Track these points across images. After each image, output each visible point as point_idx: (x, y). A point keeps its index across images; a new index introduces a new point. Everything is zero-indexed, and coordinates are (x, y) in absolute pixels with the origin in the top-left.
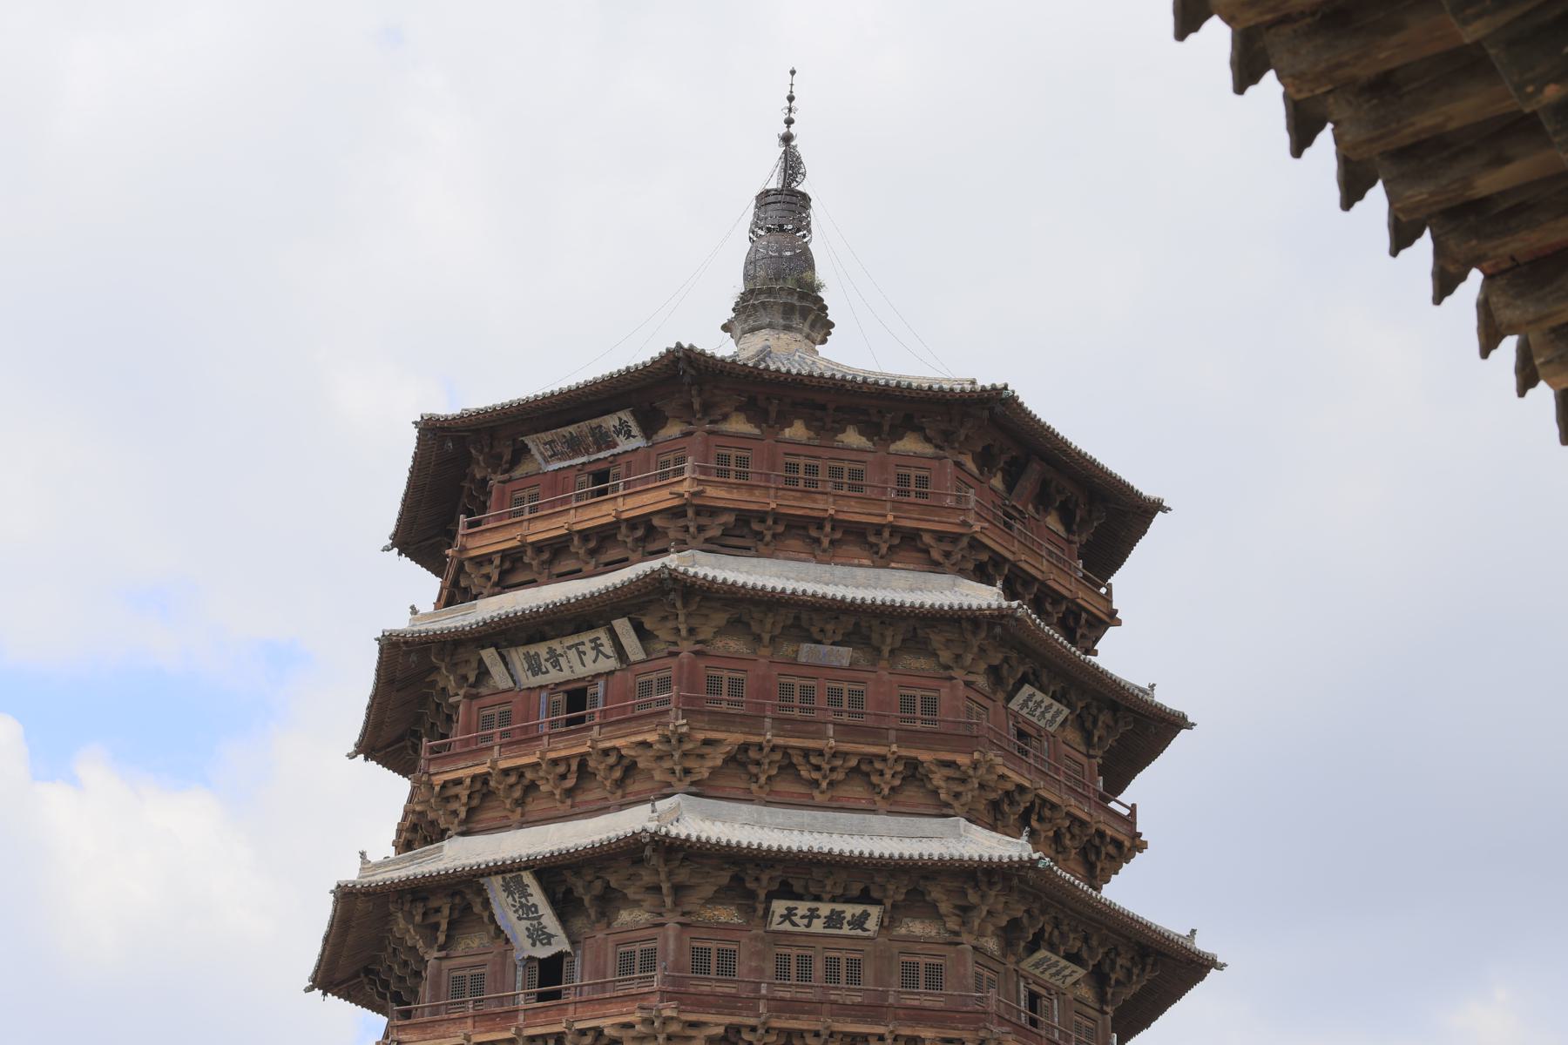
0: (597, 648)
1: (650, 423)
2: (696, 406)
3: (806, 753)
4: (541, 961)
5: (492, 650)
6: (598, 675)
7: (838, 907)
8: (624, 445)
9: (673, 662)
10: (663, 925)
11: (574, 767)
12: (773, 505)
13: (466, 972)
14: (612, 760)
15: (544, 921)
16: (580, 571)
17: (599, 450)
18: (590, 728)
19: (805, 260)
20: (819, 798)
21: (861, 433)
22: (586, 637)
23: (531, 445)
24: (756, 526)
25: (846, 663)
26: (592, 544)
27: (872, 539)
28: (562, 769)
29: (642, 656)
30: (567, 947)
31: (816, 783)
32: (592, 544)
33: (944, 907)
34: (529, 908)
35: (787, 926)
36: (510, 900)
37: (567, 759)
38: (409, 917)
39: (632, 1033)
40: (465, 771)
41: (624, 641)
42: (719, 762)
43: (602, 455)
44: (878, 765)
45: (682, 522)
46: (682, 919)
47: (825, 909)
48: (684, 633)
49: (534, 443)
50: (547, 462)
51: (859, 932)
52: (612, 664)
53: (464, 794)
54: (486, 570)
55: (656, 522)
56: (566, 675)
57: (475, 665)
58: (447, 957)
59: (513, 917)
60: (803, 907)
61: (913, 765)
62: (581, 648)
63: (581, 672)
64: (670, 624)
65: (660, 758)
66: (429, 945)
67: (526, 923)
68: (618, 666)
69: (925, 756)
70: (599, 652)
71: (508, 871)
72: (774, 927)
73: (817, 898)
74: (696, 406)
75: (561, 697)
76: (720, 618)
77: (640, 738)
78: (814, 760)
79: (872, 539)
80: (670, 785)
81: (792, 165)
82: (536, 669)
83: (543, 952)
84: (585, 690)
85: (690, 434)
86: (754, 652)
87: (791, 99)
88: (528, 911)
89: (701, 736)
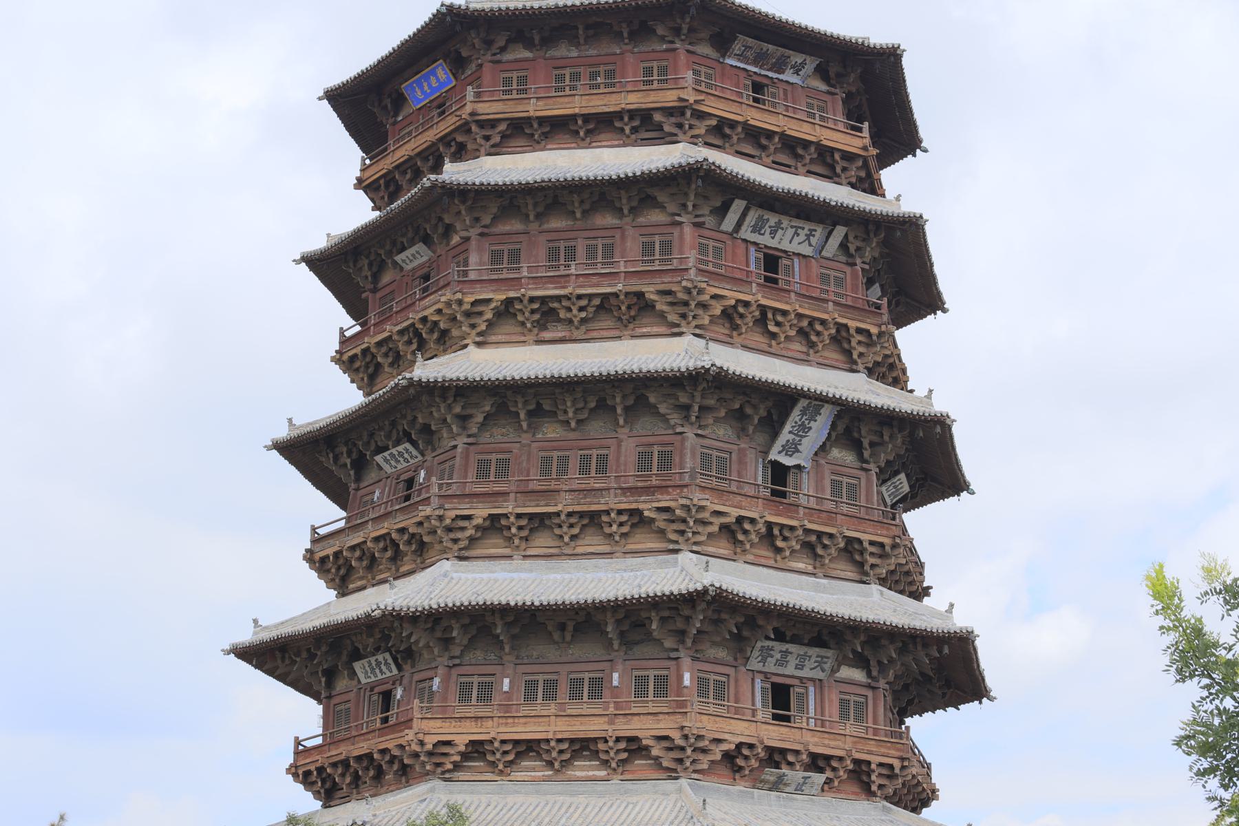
0: (808, 237)
4: (776, 465)
5: (744, 203)
6: (799, 255)
8: (789, 76)
9: (848, 270)
10: (867, 470)
13: (715, 453)
15: (804, 440)
16: (753, 157)
18: (826, 301)
22: (808, 226)
36: (797, 419)
37: (800, 316)
38: (703, 397)
40: (732, 295)
41: (830, 240)
43: (770, 74)
45: (845, 164)
52: (806, 250)
62: (800, 231)
63: (785, 245)
64: (859, 244)
65: (859, 342)
67: (791, 437)
70: (808, 239)
71: (819, 400)
75: (761, 256)
80: (855, 363)
83: (788, 461)
84: (777, 259)
88: (803, 429)
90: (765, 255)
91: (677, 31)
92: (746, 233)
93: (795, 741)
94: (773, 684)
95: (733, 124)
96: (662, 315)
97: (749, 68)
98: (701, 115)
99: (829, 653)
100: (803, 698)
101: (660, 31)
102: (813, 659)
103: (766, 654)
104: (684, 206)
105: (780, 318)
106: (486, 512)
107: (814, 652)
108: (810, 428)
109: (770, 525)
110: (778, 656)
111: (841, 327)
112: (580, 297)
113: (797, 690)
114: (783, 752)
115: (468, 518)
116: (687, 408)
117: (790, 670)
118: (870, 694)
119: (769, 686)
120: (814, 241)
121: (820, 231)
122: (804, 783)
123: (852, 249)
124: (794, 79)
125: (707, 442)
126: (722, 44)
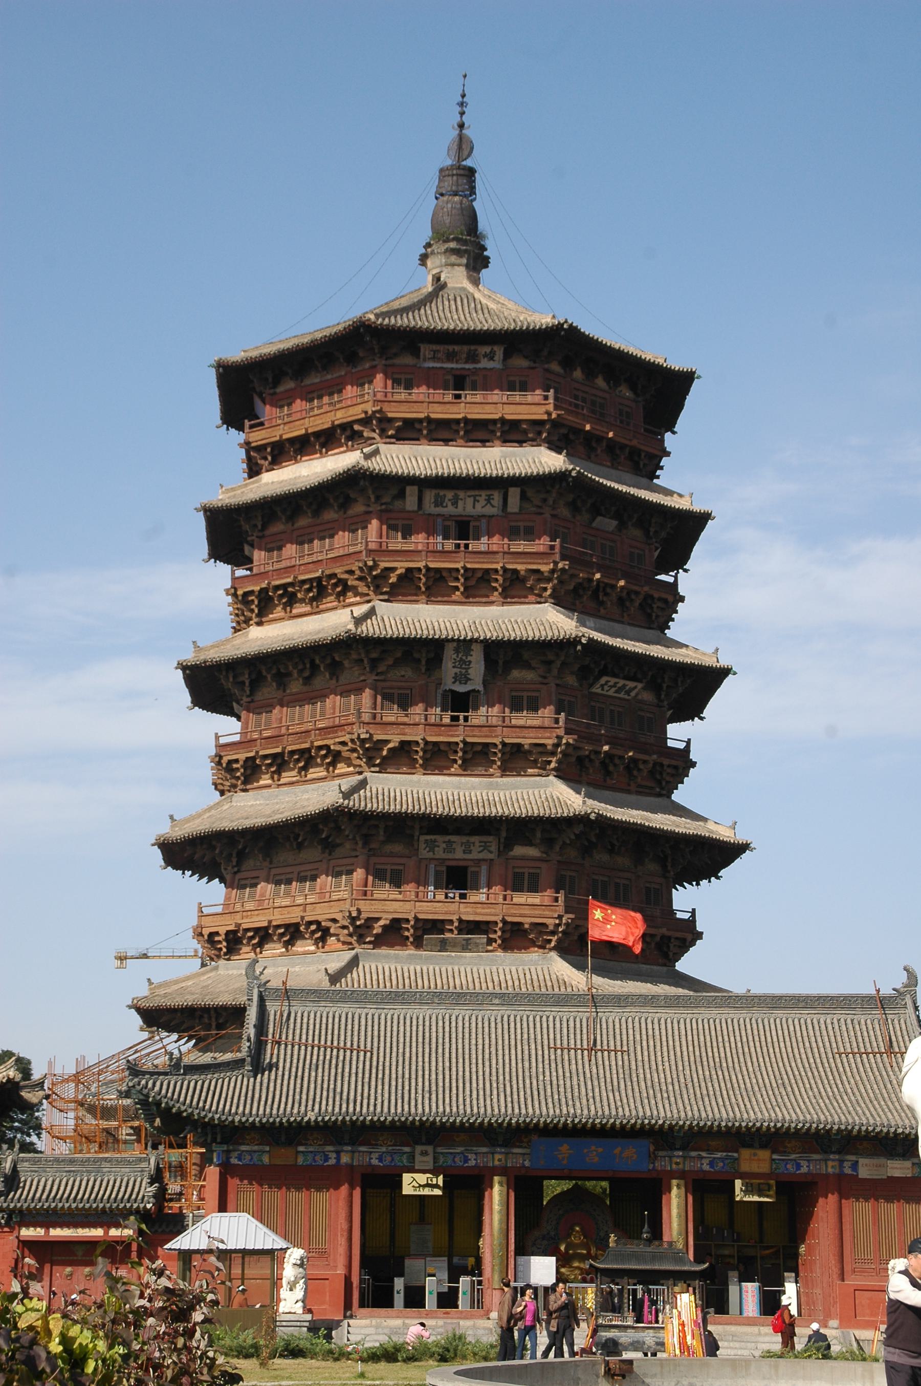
0: (489, 500)
1: (507, 356)
3: (606, 584)
5: (416, 488)
6: (484, 516)
7: (627, 682)
8: (485, 364)
11: (479, 575)
12: (588, 427)
14: (509, 575)
17: (466, 362)
19: (473, 218)
20: (602, 611)
21: (605, 379)
22: (484, 493)
23: (422, 350)
24: (571, 437)
25: (611, 529)
26: (470, 427)
27: (618, 452)
28: (470, 574)
29: (516, 510)
30: (481, 688)
31: (602, 603)
32: (470, 427)
33: (665, 686)
34: (465, 662)
35: (599, 691)
36: (454, 656)
37: (474, 570)
38: (367, 652)
39: (540, 749)
41: (510, 500)
42: (571, 587)
43: (467, 366)
44: (633, 597)
45: (538, 428)
46: (558, 682)
47: (621, 682)
48: (551, 502)
49: (426, 349)
50: (425, 360)
51: (626, 697)
53: (393, 579)
54: (383, 426)
56: (459, 510)
57: (394, 491)
58: (384, 681)
59: (450, 665)
60: (613, 680)
61: (649, 597)
63: (470, 510)
66: (371, 672)
67: (457, 670)
68: (500, 513)
69: (656, 595)
72: (594, 690)
73: (615, 675)
76: (570, 497)
77: (534, 567)
78: (608, 590)
79: (618, 452)
81: (463, 145)
82: (439, 503)
83: (461, 688)
84: (469, 522)
85: (533, 368)
86: (574, 517)
87: (463, 96)
88: (465, 664)
89: (572, 572)
90: (456, 521)
92: (430, 507)
93: (446, 913)
94: (448, 867)
95: (420, 421)
96: (354, 589)
97: (445, 365)
98: (391, 420)
99: (491, 838)
100: (477, 875)
101: (361, 354)
102: (477, 844)
103: (432, 846)
105: (454, 574)
106: (242, 756)
107: (475, 839)
108: (470, 662)
109: (436, 744)
110: (444, 845)
111: (515, 571)
112: (304, 582)
113: (473, 869)
114: (443, 921)
115: (237, 761)
116: (362, 661)
117: (459, 854)
118: (544, 865)
119: (444, 869)
120: (495, 503)
121: (497, 497)
122: (468, 944)
124: (490, 365)
125: (388, 684)
126: (416, 353)
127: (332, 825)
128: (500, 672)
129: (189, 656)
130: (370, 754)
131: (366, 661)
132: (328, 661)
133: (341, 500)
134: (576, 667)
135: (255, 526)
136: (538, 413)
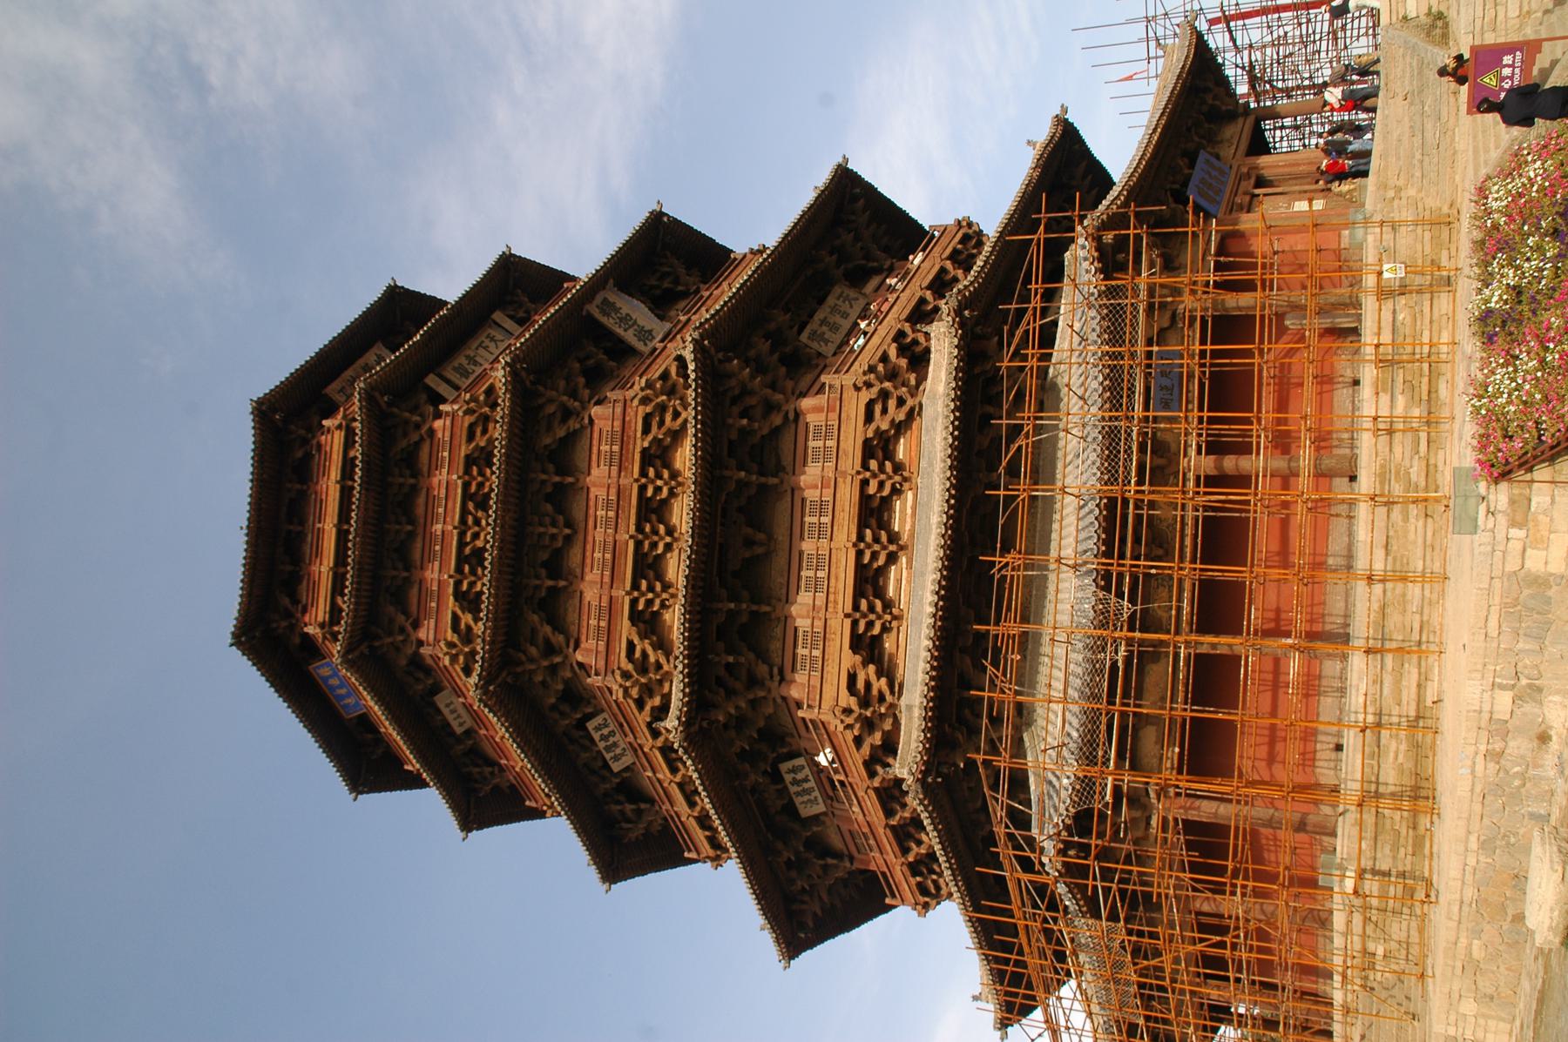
2: (302, 432)
28: (470, 520)
33: (666, 285)
37: (464, 511)
38: (532, 660)
53: (466, 618)
55: (352, 454)
74: (302, 432)
91: (292, 627)
101: (297, 640)
104: (404, 641)
123: (415, 437)
127: (733, 733)
128: (571, 480)
129: (593, 874)
130: (652, 669)
131: (545, 663)
132: (566, 708)
133: (421, 675)
134: (582, 380)
135: (492, 773)
136: (338, 438)
